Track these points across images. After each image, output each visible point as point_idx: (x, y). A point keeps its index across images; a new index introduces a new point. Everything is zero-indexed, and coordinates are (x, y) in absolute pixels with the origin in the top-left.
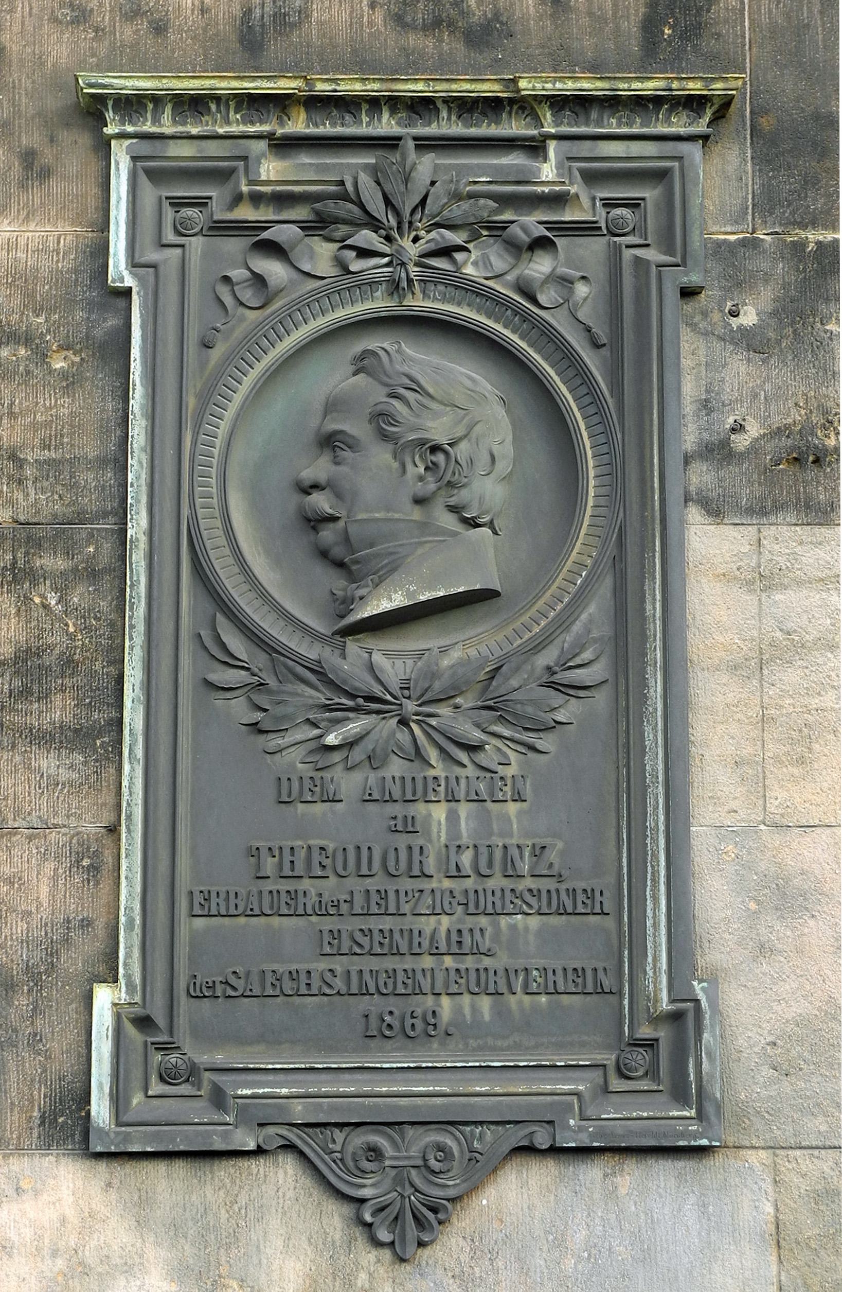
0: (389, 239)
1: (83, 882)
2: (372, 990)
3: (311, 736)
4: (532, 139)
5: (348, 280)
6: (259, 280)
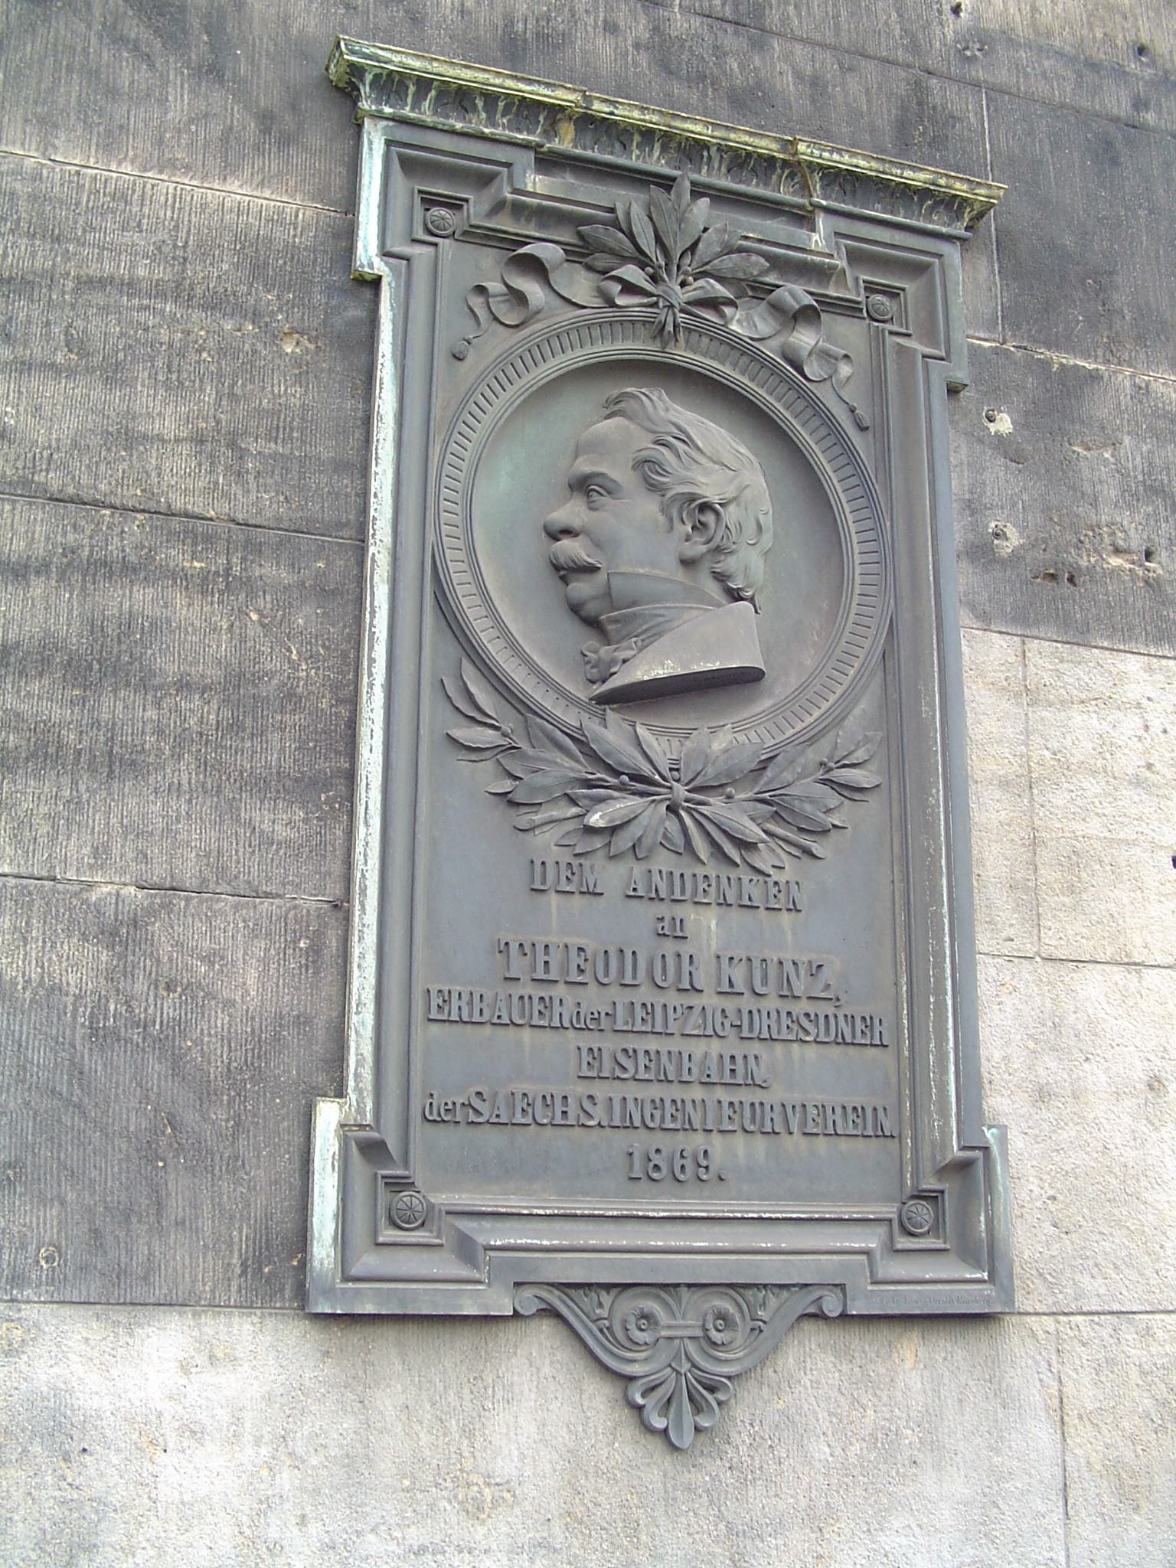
0: (654, 279)
1: (300, 967)
2: (637, 1123)
3: (569, 815)
4: (801, 207)
5: (609, 313)
6: (518, 298)
